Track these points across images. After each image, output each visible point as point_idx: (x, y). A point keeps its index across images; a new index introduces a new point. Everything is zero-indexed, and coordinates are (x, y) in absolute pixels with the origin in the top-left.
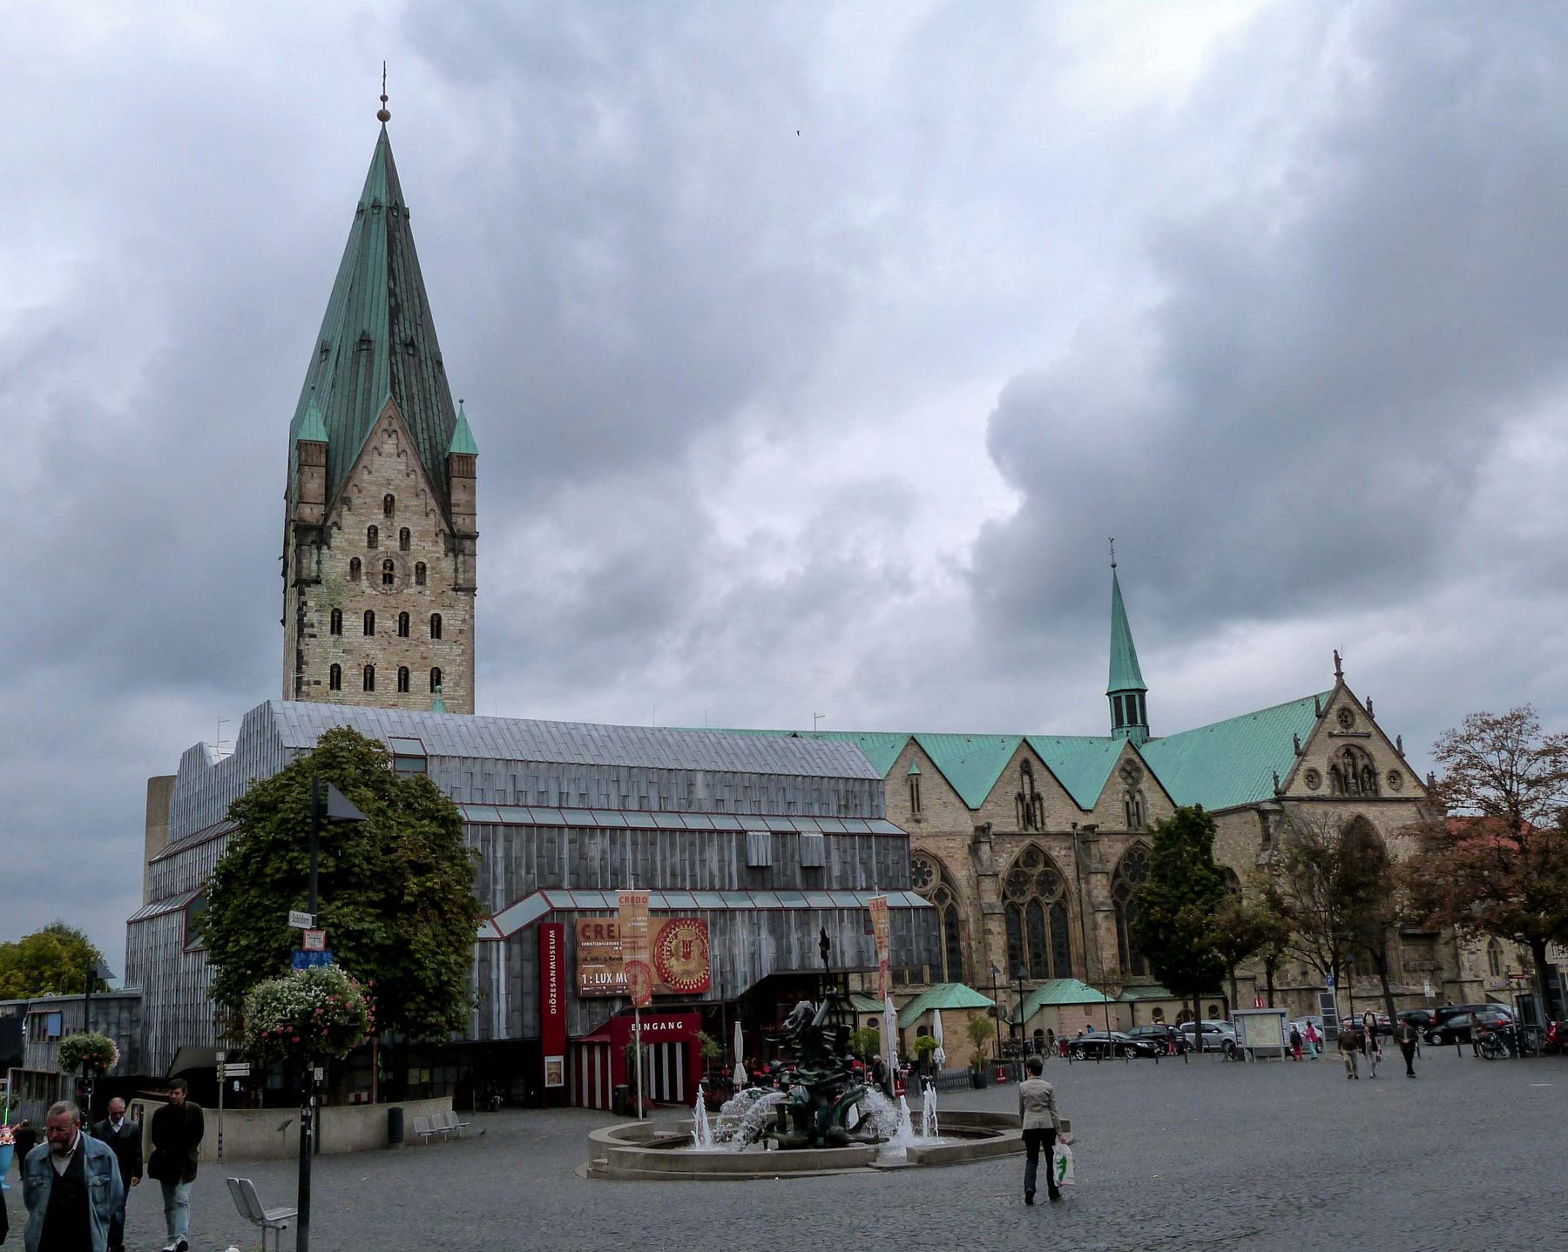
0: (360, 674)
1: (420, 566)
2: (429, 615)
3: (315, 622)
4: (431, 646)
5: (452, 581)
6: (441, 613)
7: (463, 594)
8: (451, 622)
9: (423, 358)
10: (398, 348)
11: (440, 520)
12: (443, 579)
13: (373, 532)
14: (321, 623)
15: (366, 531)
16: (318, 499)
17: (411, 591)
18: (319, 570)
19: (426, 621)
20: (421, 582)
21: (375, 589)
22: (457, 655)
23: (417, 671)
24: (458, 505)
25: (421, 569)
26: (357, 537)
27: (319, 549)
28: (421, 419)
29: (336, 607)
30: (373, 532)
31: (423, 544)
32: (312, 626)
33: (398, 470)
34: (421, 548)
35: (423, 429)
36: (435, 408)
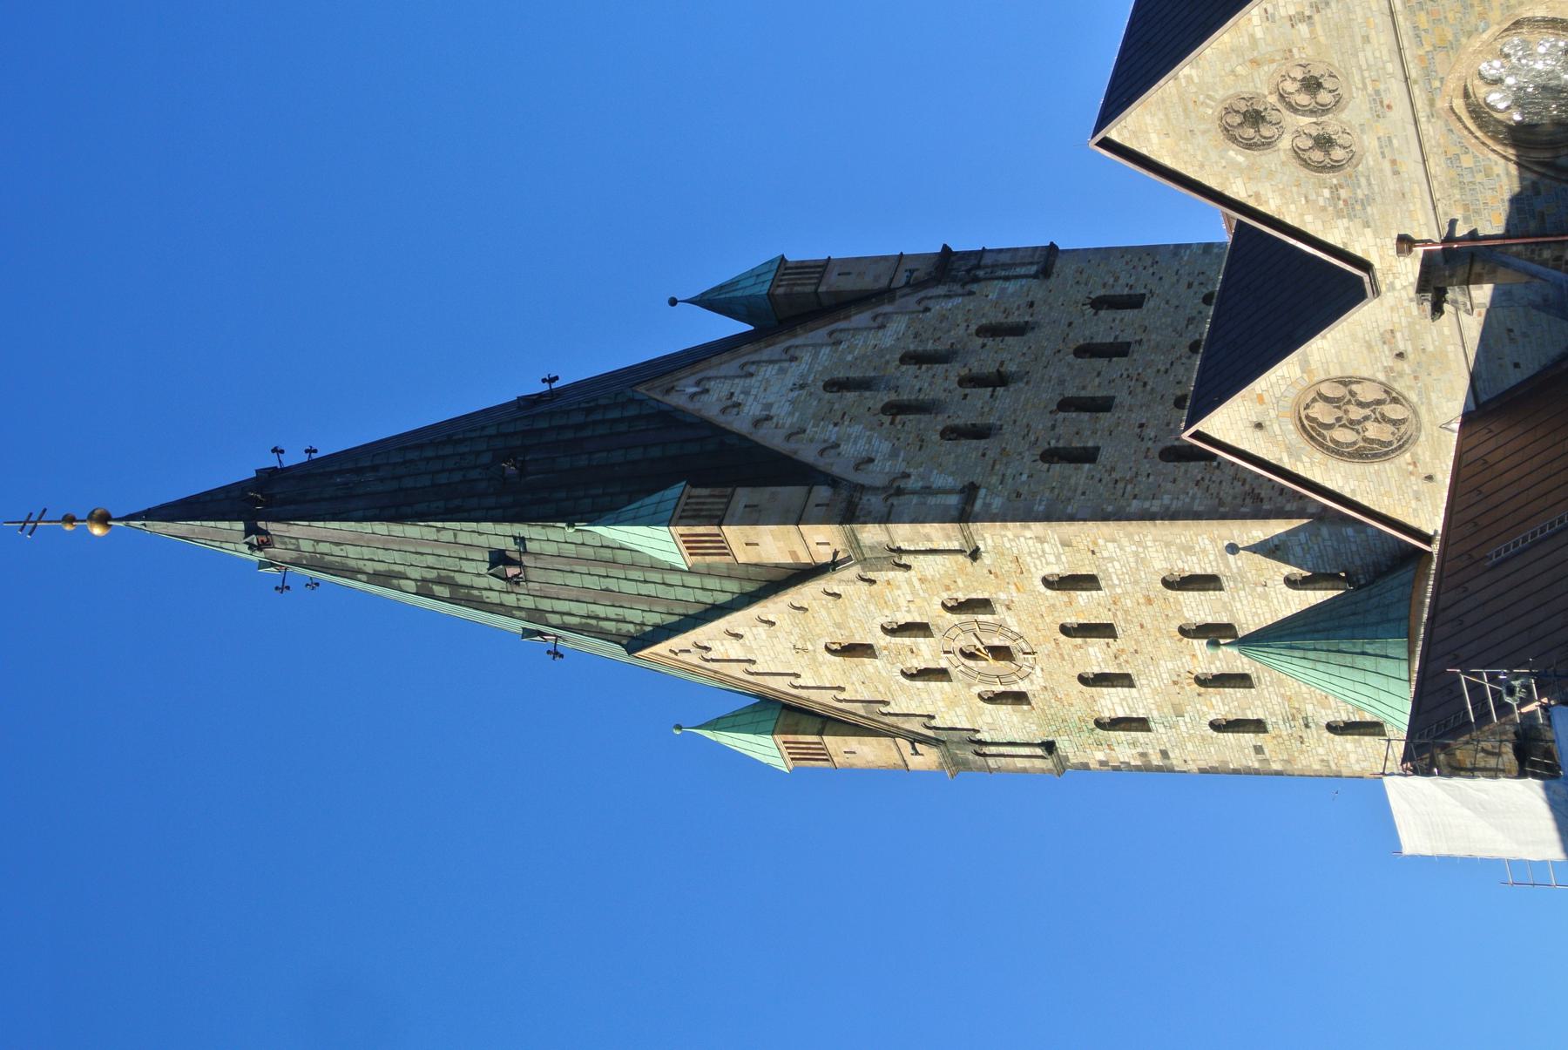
2: (1049, 593)
3: (1134, 752)
8: (1052, 559)
10: (528, 603)
14: (1134, 744)
20: (984, 605)
31: (903, 602)
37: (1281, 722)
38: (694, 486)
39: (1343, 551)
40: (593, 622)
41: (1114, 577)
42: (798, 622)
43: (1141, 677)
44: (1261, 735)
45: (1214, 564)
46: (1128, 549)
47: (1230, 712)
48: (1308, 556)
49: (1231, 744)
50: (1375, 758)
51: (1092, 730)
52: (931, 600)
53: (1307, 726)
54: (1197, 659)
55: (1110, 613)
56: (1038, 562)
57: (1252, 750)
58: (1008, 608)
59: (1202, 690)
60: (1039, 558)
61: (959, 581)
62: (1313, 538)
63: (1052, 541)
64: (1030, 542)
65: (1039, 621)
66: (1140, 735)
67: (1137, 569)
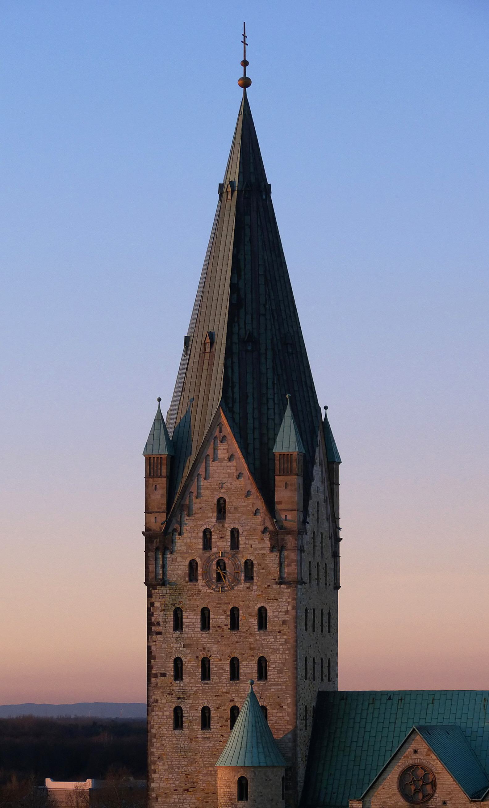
0: (198, 666)
1: (249, 563)
2: (256, 608)
3: (160, 620)
4: (258, 637)
5: (277, 575)
6: (268, 608)
7: (286, 587)
8: (276, 614)
9: (263, 351)
11: (265, 519)
12: (270, 574)
13: (207, 535)
15: (201, 535)
16: (161, 508)
17: (240, 587)
18: (164, 573)
19: (253, 614)
20: (249, 577)
21: (209, 588)
22: (282, 645)
23: (246, 661)
24: (280, 503)
25: (249, 565)
26: (194, 541)
27: (164, 554)
28: (254, 418)
29: (177, 606)
30: (207, 535)
31: (251, 542)
32: (158, 624)
33: (229, 473)
34: (249, 546)
35: (254, 429)
36: (271, 403)
37: (181, 688)
38: (303, 456)
39: (279, 732)
40: (230, 385)
41: (266, 638)
42: (238, 490)
43: (207, 635)
44: (173, 678)
45: (273, 680)
46: (281, 647)
47: (187, 668)
48: (276, 718)
49: (167, 664)
50: (160, 723)
51: (174, 605)
52: (253, 555)
53: (179, 698)
54: (219, 661)
55: (245, 631)
56: (274, 608)
57: (164, 672)
58: (247, 588)
59: (200, 659)
60: (276, 609)
61: (264, 571)
62: (286, 722)
63: (286, 617)
64: (286, 607)
65: (240, 600)
66: (172, 624)
67: (270, 648)
